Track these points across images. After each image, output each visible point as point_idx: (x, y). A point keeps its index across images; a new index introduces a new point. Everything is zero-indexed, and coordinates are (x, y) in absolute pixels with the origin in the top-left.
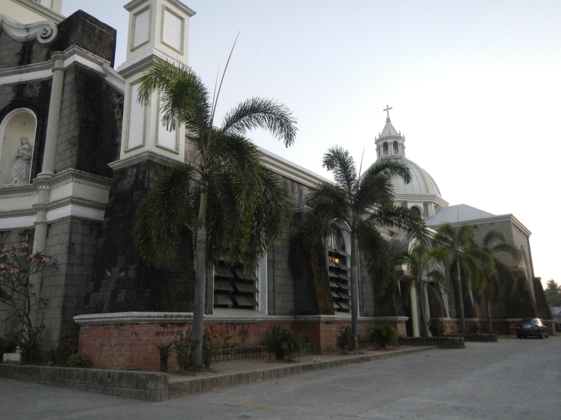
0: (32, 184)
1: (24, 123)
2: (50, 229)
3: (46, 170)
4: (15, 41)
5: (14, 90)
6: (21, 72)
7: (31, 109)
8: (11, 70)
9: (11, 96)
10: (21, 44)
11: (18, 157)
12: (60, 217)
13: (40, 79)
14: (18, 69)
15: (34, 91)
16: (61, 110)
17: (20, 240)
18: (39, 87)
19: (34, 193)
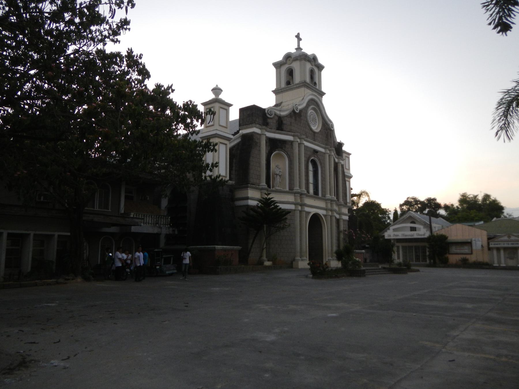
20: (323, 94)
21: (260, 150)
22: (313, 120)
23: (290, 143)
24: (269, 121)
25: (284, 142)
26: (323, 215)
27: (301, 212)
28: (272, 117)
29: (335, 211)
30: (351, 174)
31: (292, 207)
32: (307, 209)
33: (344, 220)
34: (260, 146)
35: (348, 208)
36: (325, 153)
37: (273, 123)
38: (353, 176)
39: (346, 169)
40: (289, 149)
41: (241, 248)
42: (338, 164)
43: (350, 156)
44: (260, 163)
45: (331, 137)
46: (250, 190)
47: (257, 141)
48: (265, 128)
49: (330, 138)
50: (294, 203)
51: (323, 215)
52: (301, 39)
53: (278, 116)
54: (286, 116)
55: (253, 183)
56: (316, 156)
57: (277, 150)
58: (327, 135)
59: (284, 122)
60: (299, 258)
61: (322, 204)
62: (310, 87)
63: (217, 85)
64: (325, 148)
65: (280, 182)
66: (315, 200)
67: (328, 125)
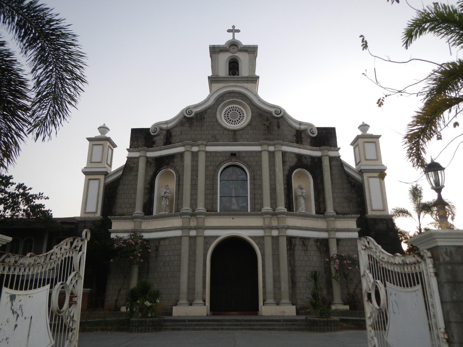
0: (322, 215)
1: (299, 177)
2: (340, 242)
3: (330, 210)
4: (291, 127)
5: (296, 157)
6: (299, 148)
7: (309, 172)
8: (290, 144)
9: (295, 160)
10: (295, 131)
11: (302, 196)
12: (347, 237)
13: (310, 155)
14: (299, 146)
15: (307, 161)
16: (332, 179)
17: (316, 244)
18: (310, 160)
19: (319, 219)
20: (255, 79)
21: (137, 175)
22: (234, 117)
23: (180, 156)
24: (156, 139)
25: (171, 157)
26: (251, 237)
27: (193, 239)
28: (156, 134)
29: (289, 228)
30: (384, 165)
31: (178, 233)
32: (208, 233)
33: (338, 240)
34: (138, 171)
35: (356, 219)
36: (261, 152)
37: (159, 140)
38: (386, 167)
39: (367, 160)
40: (178, 163)
41: (90, 291)
42: (323, 158)
43: (380, 139)
44: (135, 189)
45: (279, 127)
46: (114, 222)
47: (132, 166)
48: (140, 149)
49: (276, 128)
50: (178, 228)
51: (253, 238)
52: (238, 30)
53: (166, 130)
54: (176, 126)
55: (121, 214)
56: (235, 160)
57: (162, 168)
58: (268, 127)
59: (173, 134)
60: (185, 301)
61: (257, 221)
62: (222, 79)
63: (104, 124)
64: (260, 145)
65: (166, 205)
66: (233, 218)
67: (271, 113)
